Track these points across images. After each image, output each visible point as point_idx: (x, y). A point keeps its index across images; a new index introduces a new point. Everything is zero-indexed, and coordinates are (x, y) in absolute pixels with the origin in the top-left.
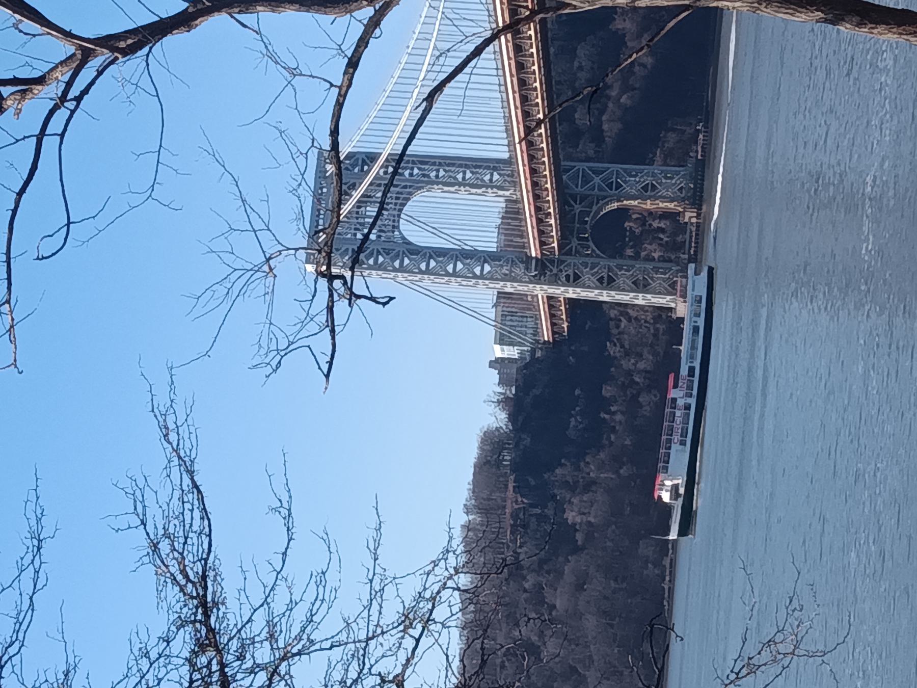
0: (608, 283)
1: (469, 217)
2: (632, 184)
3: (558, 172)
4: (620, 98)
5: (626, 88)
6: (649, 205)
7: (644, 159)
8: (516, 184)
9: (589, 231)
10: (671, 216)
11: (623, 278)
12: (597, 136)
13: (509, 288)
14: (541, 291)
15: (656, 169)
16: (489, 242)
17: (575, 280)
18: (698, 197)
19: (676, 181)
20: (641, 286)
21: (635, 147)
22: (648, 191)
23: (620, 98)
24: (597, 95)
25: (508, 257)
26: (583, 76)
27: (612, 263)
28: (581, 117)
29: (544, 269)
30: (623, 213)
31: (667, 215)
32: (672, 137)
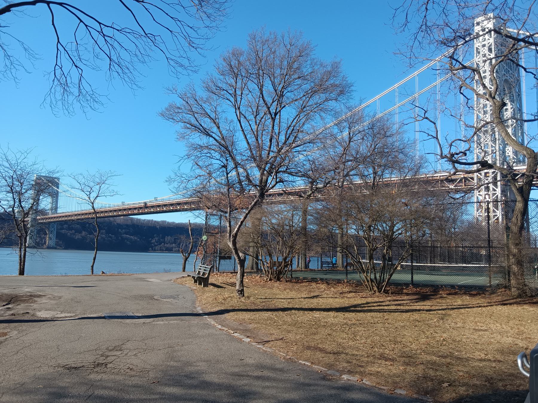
4: (69, 233)
6: (47, 239)
7: (57, 237)
10: (45, 243)
12: (62, 229)
15: (55, 240)
18: (49, 248)
19: (52, 243)
21: (59, 236)
22: (50, 238)
23: (69, 233)
24: (70, 229)
26: (74, 226)
27: (35, 232)
31: (45, 242)
32: (61, 243)
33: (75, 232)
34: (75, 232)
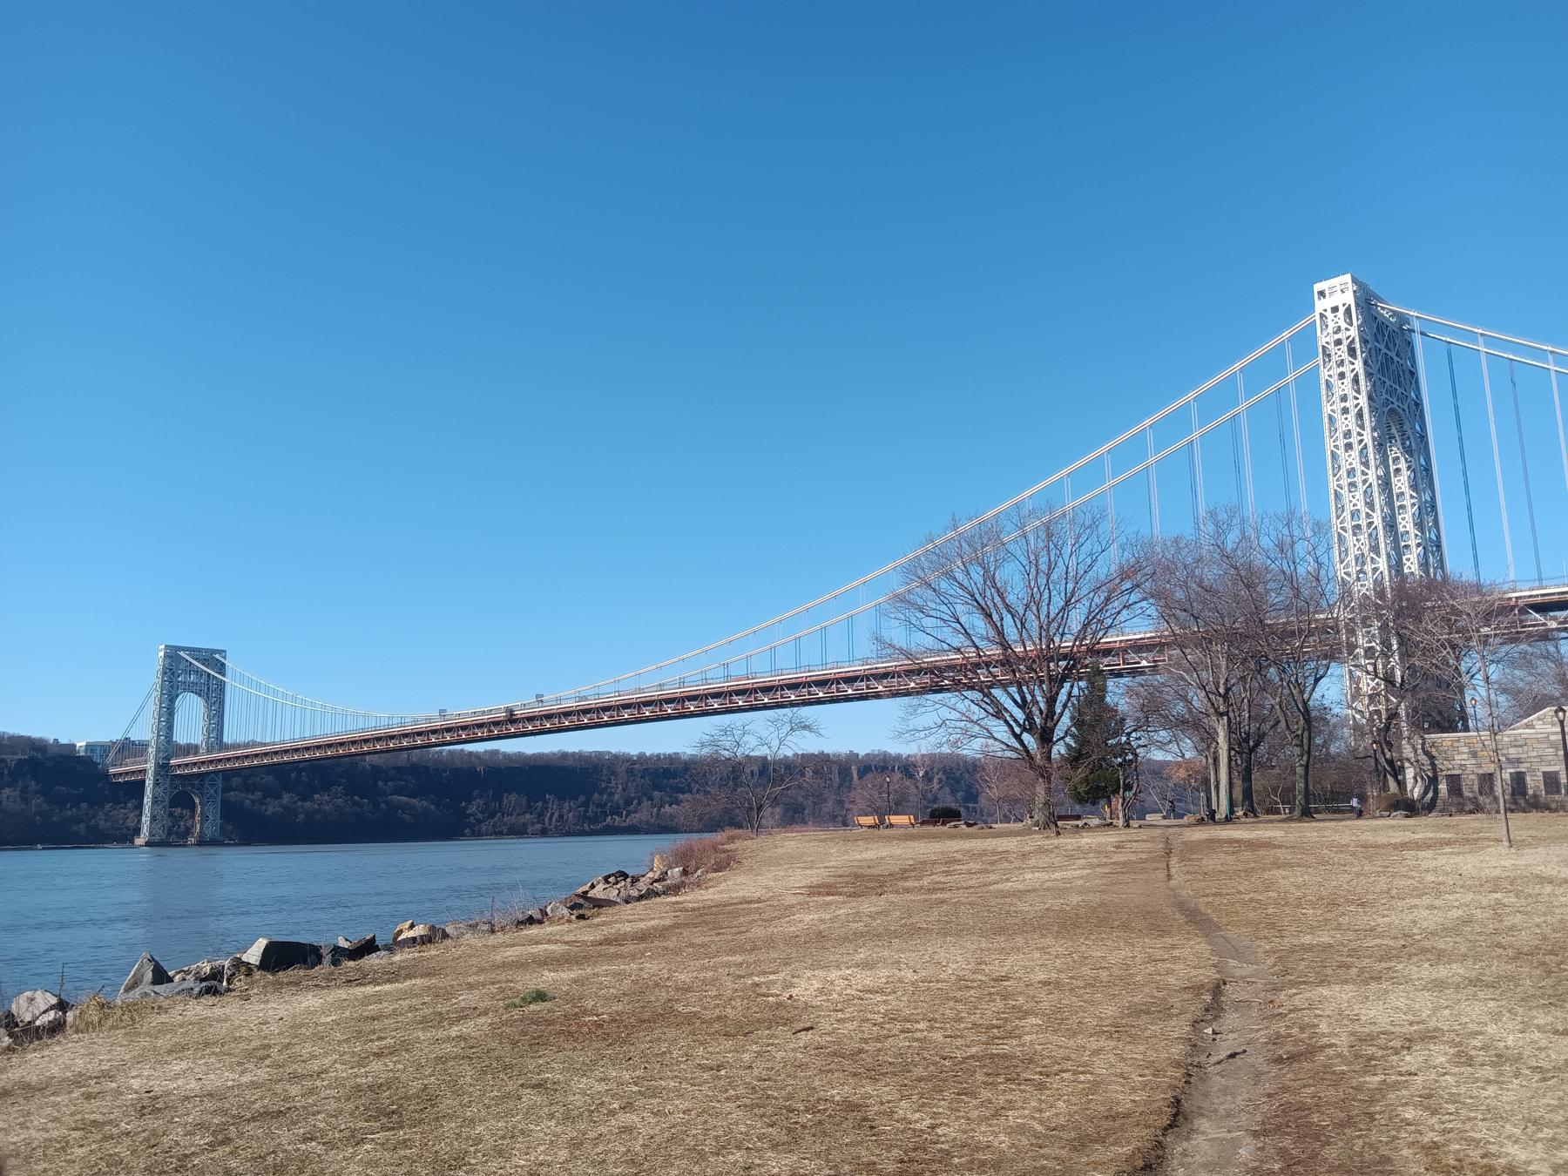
0: (155, 801)
1: (191, 724)
2: (210, 809)
3: (216, 772)
4: (248, 799)
5: (253, 802)
8: (209, 751)
9: (183, 789)
11: (160, 811)
13: (152, 750)
14: (150, 766)
16: (181, 737)
17: (156, 783)
18: (202, 843)
20: (153, 818)
22: (205, 818)
24: (248, 787)
25: (169, 748)
28: (236, 781)
29: (163, 768)
30: (193, 807)
33: (265, 797)
34: (265, 797)
